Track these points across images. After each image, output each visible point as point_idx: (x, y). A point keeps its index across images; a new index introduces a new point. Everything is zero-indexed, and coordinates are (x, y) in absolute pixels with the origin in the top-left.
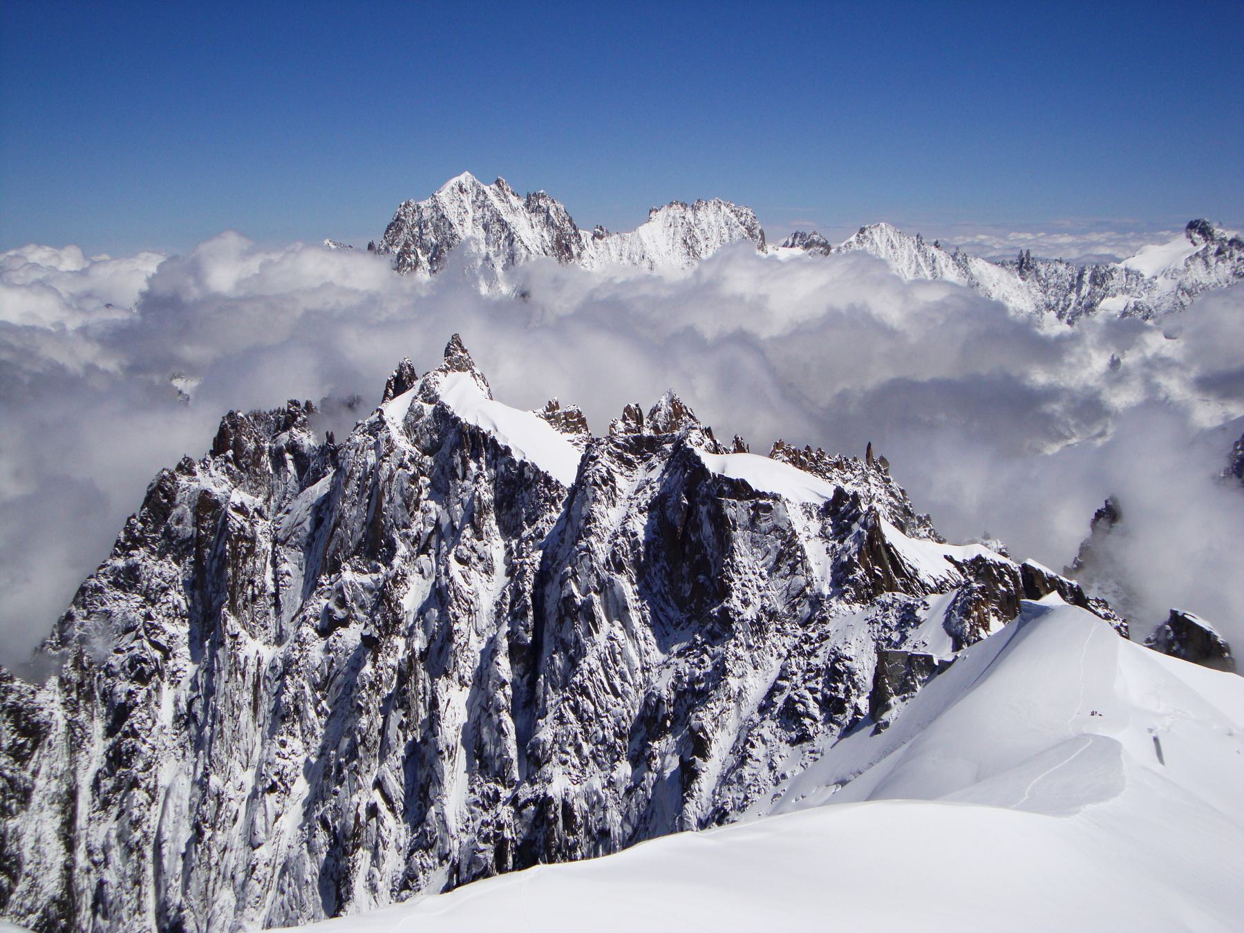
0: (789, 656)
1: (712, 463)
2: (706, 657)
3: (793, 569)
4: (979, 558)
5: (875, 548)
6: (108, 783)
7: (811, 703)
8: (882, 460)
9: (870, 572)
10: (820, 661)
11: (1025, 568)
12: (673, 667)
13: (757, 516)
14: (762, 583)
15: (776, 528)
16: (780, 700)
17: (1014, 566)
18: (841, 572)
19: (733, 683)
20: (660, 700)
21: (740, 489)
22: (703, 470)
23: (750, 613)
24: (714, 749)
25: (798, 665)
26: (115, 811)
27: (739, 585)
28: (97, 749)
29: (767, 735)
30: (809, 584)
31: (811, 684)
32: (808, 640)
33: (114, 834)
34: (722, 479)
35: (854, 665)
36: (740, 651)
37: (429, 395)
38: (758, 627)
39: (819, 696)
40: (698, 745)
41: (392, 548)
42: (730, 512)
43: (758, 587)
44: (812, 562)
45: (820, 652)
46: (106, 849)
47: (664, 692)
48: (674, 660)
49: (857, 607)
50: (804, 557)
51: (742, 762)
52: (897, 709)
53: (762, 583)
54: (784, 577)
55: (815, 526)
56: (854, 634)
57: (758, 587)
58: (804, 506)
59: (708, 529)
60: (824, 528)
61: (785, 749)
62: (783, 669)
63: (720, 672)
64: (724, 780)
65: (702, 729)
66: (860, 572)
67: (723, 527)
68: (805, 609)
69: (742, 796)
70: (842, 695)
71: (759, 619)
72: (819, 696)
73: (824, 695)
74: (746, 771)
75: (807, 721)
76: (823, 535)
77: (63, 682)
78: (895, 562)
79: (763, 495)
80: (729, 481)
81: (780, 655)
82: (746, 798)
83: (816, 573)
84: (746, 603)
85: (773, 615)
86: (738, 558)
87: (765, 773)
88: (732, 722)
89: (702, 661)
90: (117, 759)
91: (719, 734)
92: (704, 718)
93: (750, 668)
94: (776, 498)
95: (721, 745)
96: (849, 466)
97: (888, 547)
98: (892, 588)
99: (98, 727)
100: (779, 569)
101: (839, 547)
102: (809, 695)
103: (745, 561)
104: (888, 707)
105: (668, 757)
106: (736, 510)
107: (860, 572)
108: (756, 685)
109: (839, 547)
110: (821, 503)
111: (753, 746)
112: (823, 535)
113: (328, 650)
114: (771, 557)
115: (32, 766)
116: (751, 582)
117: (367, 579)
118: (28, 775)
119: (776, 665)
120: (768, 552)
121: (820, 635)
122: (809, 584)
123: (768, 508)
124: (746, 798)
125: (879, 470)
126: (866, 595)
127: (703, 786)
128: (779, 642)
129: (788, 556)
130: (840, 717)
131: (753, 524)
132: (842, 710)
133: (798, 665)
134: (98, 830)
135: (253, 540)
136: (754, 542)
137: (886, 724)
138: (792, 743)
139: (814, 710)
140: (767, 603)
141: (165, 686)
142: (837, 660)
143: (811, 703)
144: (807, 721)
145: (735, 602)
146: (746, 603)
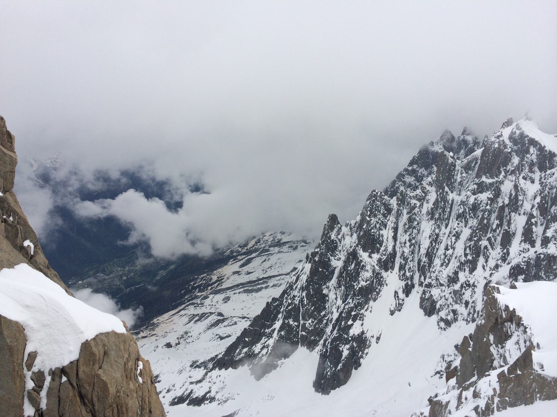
6: (407, 226)
26: (408, 234)
28: (405, 218)
33: (407, 240)
37: (518, 128)
41: (500, 173)
46: (405, 243)
77: (398, 198)
90: (411, 220)
99: (405, 212)
113: (475, 199)
115: (388, 218)
117: (490, 181)
118: (386, 221)
134: (403, 237)
135: (455, 166)
141: (425, 203)
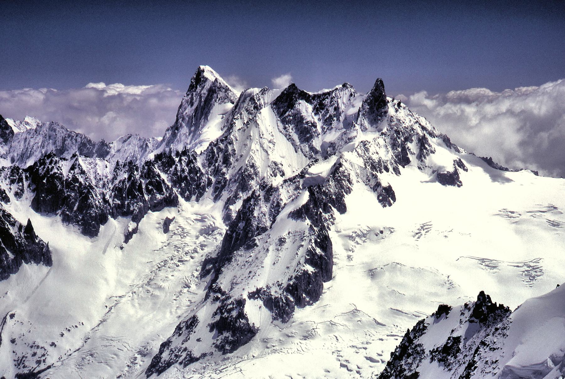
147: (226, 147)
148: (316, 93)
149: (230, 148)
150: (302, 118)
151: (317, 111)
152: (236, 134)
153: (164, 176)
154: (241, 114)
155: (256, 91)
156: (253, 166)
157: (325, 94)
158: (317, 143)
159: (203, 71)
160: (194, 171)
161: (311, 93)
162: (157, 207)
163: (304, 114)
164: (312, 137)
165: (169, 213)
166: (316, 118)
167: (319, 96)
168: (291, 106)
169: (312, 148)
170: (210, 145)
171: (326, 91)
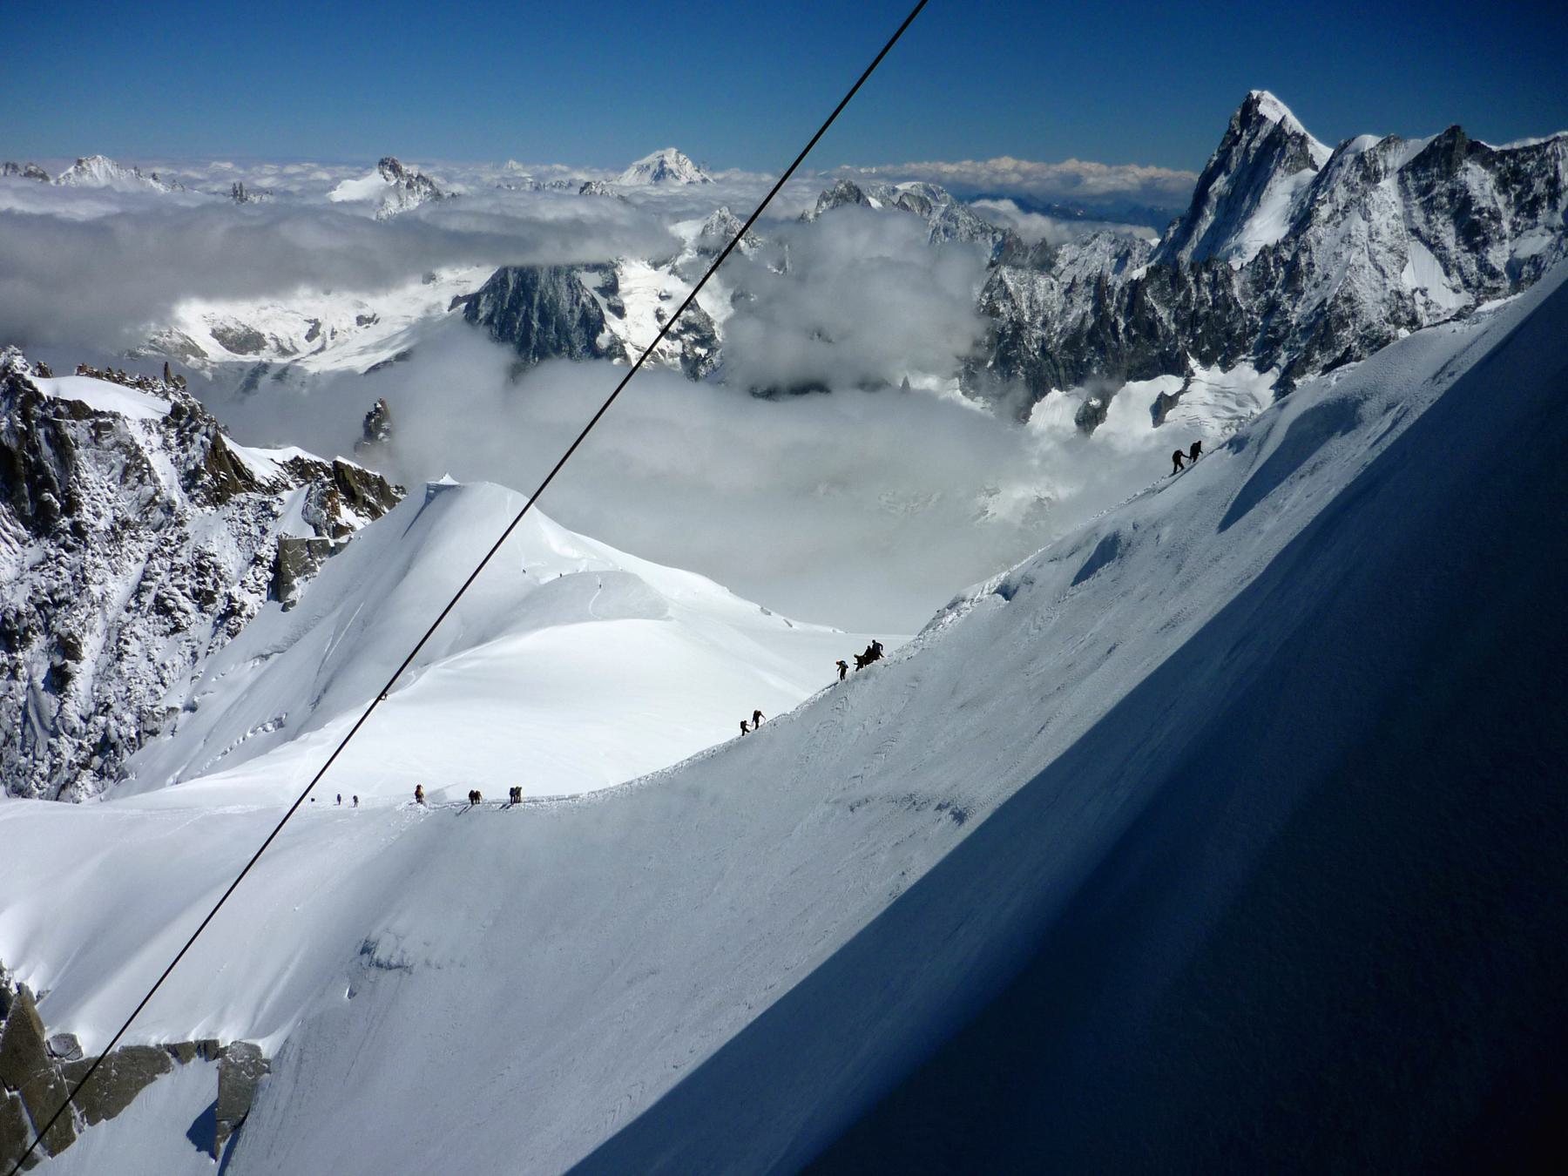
0: (150, 557)
1: (44, 387)
2: (62, 569)
3: (141, 480)
4: (297, 458)
5: (218, 456)
7: (181, 598)
8: (179, 378)
9: (215, 477)
10: (185, 558)
11: (336, 464)
12: (27, 583)
13: (98, 434)
14: (111, 496)
15: (118, 444)
16: (148, 599)
17: (328, 464)
18: (190, 479)
19: (96, 590)
20: (18, 615)
21: (78, 410)
22: (36, 396)
23: (102, 525)
24: (85, 651)
25: (161, 567)
27: (87, 499)
29: (139, 631)
30: (157, 493)
31: (178, 581)
32: (168, 542)
34: (53, 402)
35: (219, 560)
36: (98, 560)
38: (114, 536)
39: (187, 591)
40: (68, 648)
42: (70, 432)
43: (108, 500)
44: (158, 473)
45: (183, 552)
47: (23, 607)
48: (29, 575)
49: (208, 509)
50: (150, 469)
51: (119, 658)
52: (300, 588)
53: (111, 496)
54: (133, 488)
55: (156, 440)
56: (217, 535)
57: (108, 500)
58: (143, 422)
59: (46, 450)
60: (165, 441)
61: (161, 642)
62: (145, 571)
63: (81, 580)
64: (101, 677)
65: (71, 635)
66: (207, 477)
67: (63, 447)
68: (157, 516)
69: (124, 689)
70: (211, 588)
71: (113, 529)
72: (187, 591)
73: (193, 590)
74: (124, 666)
75: (179, 614)
76: (166, 446)
78: (238, 468)
79: (102, 414)
80: (64, 402)
81: (138, 560)
82: (129, 690)
83: (163, 482)
84: (98, 515)
85: (126, 524)
86: (83, 475)
87: (144, 665)
88: (99, 625)
89: (58, 573)
91: (87, 638)
92: (66, 623)
93: (110, 576)
94: (115, 416)
95: (91, 646)
96: (150, 385)
97: (229, 454)
98: (237, 490)
100: (126, 482)
101: (183, 457)
102: (176, 590)
103: (91, 477)
104: (293, 588)
105: (35, 666)
106: (76, 430)
107: (207, 477)
108: (118, 589)
109: (183, 457)
110: (159, 418)
111: (126, 643)
112: (166, 446)
114: (118, 471)
116: (99, 492)
119: (134, 571)
120: (112, 467)
121: (179, 538)
122: (157, 493)
123: (109, 426)
124: (129, 690)
125: (177, 387)
126: (218, 497)
127: (79, 686)
128: (137, 549)
129: (134, 467)
130: (211, 607)
131: (96, 440)
132: (213, 600)
133: (161, 567)
136: (98, 459)
137: (293, 603)
138: (166, 634)
139: (188, 605)
140: (119, 514)
142: (201, 557)
143: (181, 598)
144: (179, 614)
145: (86, 516)
146: (98, 515)
147: (1295, 256)
148: (1507, 147)
149: (1303, 260)
150: (1467, 201)
151: (1503, 185)
152: (1320, 232)
153: (1163, 313)
154: (1332, 192)
155: (1369, 141)
156: (1349, 299)
157: (1527, 149)
158: (1498, 257)
159: (1258, 101)
160: (1225, 303)
161: (1494, 148)
162: (1146, 372)
163: (1475, 190)
164: (1486, 242)
165: (1169, 384)
166: (1501, 200)
167: (1513, 154)
168: (1448, 174)
169: (1484, 266)
170: (1262, 252)
171: (1533, 142)
